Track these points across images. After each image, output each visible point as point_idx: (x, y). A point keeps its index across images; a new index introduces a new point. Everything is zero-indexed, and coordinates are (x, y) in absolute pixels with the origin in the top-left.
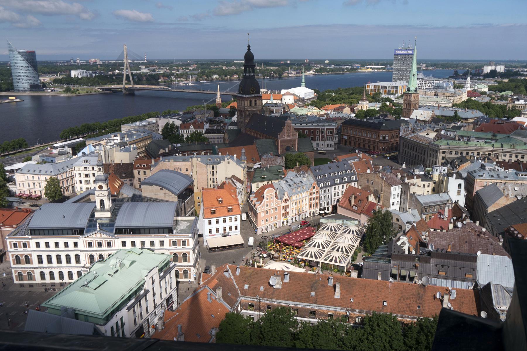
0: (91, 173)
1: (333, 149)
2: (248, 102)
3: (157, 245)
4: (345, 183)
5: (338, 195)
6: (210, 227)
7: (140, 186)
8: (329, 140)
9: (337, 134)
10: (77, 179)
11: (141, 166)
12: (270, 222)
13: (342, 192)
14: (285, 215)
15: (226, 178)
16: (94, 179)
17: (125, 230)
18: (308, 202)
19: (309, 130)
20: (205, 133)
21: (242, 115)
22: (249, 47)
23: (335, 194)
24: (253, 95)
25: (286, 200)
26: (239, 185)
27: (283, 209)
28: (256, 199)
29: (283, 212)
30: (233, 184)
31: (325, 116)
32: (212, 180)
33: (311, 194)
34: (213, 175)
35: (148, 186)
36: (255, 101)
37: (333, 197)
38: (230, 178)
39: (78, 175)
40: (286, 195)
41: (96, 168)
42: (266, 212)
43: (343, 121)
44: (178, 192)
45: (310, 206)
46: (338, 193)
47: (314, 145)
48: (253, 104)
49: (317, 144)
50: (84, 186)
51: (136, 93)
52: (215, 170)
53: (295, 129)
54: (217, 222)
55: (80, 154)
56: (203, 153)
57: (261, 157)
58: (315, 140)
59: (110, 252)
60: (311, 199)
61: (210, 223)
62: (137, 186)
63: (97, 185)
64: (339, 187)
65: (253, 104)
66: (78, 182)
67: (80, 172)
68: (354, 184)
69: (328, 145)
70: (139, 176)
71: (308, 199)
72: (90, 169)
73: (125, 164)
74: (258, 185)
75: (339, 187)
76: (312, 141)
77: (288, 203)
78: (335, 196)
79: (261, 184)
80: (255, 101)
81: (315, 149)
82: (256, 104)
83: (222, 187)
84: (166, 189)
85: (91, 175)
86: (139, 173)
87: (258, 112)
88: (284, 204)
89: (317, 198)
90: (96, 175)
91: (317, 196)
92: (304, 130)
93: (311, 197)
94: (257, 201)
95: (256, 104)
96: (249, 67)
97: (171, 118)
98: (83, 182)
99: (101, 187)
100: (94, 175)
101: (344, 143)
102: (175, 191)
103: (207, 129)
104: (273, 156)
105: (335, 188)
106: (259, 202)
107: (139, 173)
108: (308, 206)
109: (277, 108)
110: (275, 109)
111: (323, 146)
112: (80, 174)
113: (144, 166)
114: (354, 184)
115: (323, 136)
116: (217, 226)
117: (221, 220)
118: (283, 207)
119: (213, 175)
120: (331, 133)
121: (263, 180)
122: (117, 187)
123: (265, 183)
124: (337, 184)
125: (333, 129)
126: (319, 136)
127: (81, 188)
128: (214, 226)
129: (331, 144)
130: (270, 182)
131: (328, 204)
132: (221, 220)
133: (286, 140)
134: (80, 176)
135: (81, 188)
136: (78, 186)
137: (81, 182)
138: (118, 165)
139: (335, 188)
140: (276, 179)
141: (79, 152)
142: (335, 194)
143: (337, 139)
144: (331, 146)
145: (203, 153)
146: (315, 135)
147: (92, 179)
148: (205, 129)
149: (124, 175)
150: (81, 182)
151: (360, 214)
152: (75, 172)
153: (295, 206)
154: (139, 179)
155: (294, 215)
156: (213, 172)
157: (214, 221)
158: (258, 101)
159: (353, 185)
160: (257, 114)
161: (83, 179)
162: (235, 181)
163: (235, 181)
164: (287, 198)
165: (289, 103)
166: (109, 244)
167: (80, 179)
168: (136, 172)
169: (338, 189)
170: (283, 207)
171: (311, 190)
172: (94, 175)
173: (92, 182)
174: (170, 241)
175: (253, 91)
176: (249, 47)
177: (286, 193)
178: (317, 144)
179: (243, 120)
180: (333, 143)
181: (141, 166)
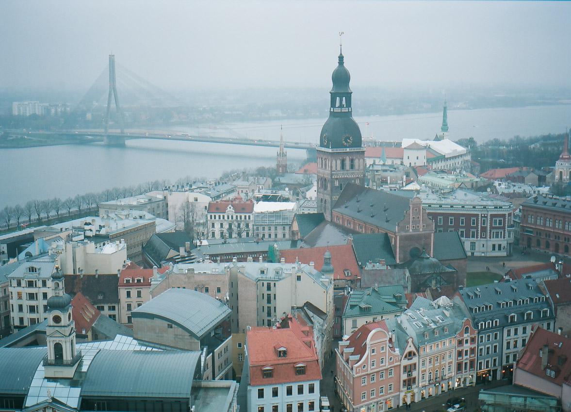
0: (39, 290)
1: (505, 254)
2: (339, 162)
4: (529, 320)
5: (515, 346)
6: (261, 402)
7: (129, 319)
8: (497, 237)
9: (512, 226)
10: (14, 302)
11: (133, 280)
12: (378, 396)
13: (524, 341)
14: (410, 383)
15: (293, 308)
16: (45, 302)
17: (98, 404)
18: (454, 359)
19: (457, 216)
21: (326, 188)
22: (341, 58)
23: (508, 343)
24: (348, 150)
25: (410, 353)
26: (317, 320)
27: (405, 371)
28: (352, 350)
29: (404, 377)
30: (306, 320)
31: (489, 190)
33: (460, 343)
34: (269, 301)
35: (145, 320)
36: (352, 161)
37: (505, 351)
38: (302, 308)
39: (15, 296)
40: (410, 343)
41: (50, 283)
42: (371, 376)
43: (522, 200)
44: (199, 335)
45: (459, 367)
46: (516, 342)
47: (467, 246)
48: (348, 166)
49: (473, 245)
50: (27, 316)
51: (128, 142)
52: (272, 293)
53: (429, 214)
54: (275, 393)
55: (22, 256)
56: (250, 258)
57: (361, 267)
58: (467, 236)
60: (460, 354)
61: (261, 394)
62: (125, 320)
63: (50, 316)
64: (516, 330)
65: (348, 166)
66: (16, 308)
67: (19, 289)
68: (549, 325)
69: (494, 246)
70: (129, 300)
71: (454, 354)
72: (40, 284)
73: (103, 276)
74: (355, 322)
75: (516, 330)
76: (463, 239)
77: (415, 360)
78: (508, 348)
79: (361, 322)
80: (352, 161)
81: (469, 254)
82: (352, 167)
83: (285, 324)
85: (40, 296)
86: (129, 294)
87: (358, 182)
88: (405, 362)
89: (472, 351)
90: (49, 296)
91: (473, 346)
92: (446, 216)
93: (460, 349)
94: (352, 354)
95: (352, 167)
96: (341, 95)
97: (192, 191)
98: (25, 309)
99: (57, 319)
101: (525, 243)
102: (195, 330)
104: (384, 268)
105: (509, 331)
106: (357, 357)
107: (129, 294)
108: (454, 367)
109: (392, 174)
110: (389, 176)
111: (484, 249)
113: (139, 281)
114: (549, 325)
115: (484, 229)
116: (276, 401)
117: (282, 390)
118: (405, 367)
119: (269, 301)
120: (500, 223)
121: (365, 311)
122: (89, 321)
123: (370, 319)
124: (513, 323)
125: (504, 216)
126: (477, 228)
127: (21, 320)
128: (268, 401)
129: (500, 246)
130: (379, 318)
131: (495, 365)
132: (282, 390)
133: (411, 236)
135: (21, 320)
136: (15, 315)
137: (21, 308)
138: (90, 278)
139: (509, 331)
140: (390, 312)
141: (19, 253)
142: (508, 343)
143: (512, 236)
144: (500, 249)
145: (250, 258)
146: (468, 227)
147: (41, 303)
149: (100, 297)
150: (21, 308)
151: (561, 386)
152: (10, 289)
153: (428, 366)
154: (129, 306)
155: (427, 383)
156: (269, 296)
157: (268, 391)
158: (356, 162)
159: (545, 327)
160: (354, 184)
161: (26, 303)
162: (311, 314)
163: (311, 314)
164: (413, 349)
165: (417, 165)
167: (20, 302)
168: (123, 292)
169: (516, 333)
170: (405, 367)
171: (461, 335)
172: (45, 295)
173: (41, 309)
175: (346, 142)
176: (341, 58)
177: (410, 340)
178: (473, 245)
179: (327, 198)
180: (504, 243)
181: (133, 280)
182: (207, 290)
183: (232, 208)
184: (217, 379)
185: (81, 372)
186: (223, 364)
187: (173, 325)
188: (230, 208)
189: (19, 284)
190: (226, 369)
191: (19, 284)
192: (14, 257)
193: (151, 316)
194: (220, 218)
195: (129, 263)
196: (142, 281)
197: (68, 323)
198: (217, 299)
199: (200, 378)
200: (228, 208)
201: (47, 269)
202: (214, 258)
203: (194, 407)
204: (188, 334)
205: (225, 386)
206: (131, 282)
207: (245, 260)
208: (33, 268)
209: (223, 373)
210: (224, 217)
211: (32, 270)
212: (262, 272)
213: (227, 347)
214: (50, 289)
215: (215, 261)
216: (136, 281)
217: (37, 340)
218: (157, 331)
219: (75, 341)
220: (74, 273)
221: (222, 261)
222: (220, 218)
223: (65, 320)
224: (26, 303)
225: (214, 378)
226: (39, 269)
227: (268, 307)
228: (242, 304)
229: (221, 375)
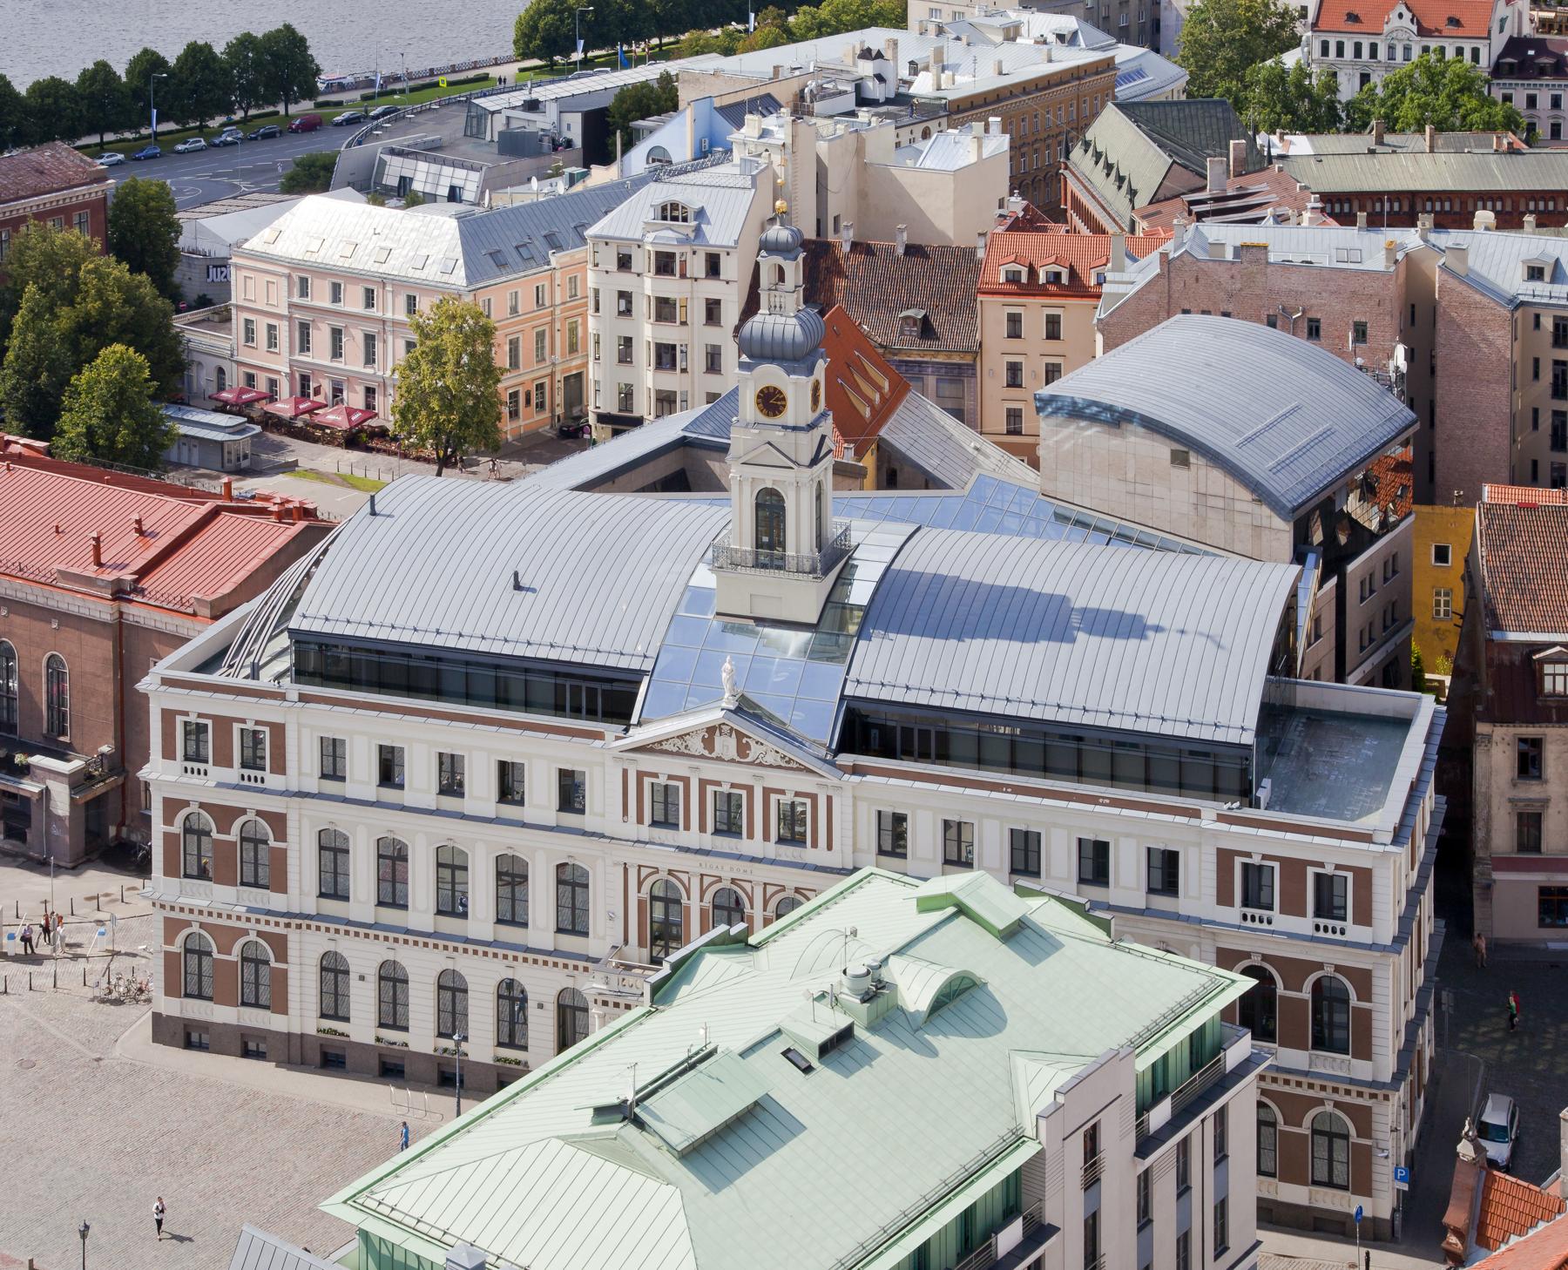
0: (691, 292)
3: (1129, 877)
20: (1498, 71)
32: (1546, 422)
56: (1484, 216)
59: (792, 879)
66: (610, 350)
72: (697, 266)
84: (1215, 458)
85: (698, 313)
99: (771, 401)
100: (713, 311)
103: (1516, 45)
112: (623, 295)
122: (867, 413)
134: (627, 312)
135: (627, 396)
141: (628, 145)
145: (1484, 216)
148: (1499, 42)
161: (647, 332)
166: (793, 828)
174: (1225, 858)
182: (1314, 331)
183: (1407, 15)
184: (1352, 679)
185: (844, 606)
186: (1377, 632)
187: (1193, 458)
188: (1401, 16)
189: (624, 263)
190: (1389, 646)
191: (624, 263)
192: (606, 159)
193: (1117, 419)
194: (1358, 54)
195: (1017, 205)
196: (1065, 280)
197: (810, 417)
198: (1360, 368)
199: (1290, 670)
200: (1394, 16)
201: (728, 207)
202: (1339, 207)
203: (1267, 782)
204: (1245, 495)
205: (1390, 714)
206: (1024, 279)
207: (1465, 222)
208: (674, 206)
209: (1376, 659)
210: (1374, 47)
211: (671, 212)
212: (1535, 273)
213: (1394, 557)
214: (734, 286)
215: (1346, 220)
216: (1042, 279)
217: (682, 471)
218: (1130, 476)
219: (829, 493)
220: (818, 234)
221: (1374, 222)
222: (1358, 54)
223: (798, 407)
224: (647, 332)
225: (1340, 676)
226: (700, 214)
227: (1556, 413)
228: (1447, 392)
229: (1367, 666)
